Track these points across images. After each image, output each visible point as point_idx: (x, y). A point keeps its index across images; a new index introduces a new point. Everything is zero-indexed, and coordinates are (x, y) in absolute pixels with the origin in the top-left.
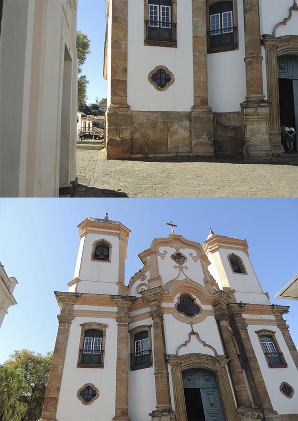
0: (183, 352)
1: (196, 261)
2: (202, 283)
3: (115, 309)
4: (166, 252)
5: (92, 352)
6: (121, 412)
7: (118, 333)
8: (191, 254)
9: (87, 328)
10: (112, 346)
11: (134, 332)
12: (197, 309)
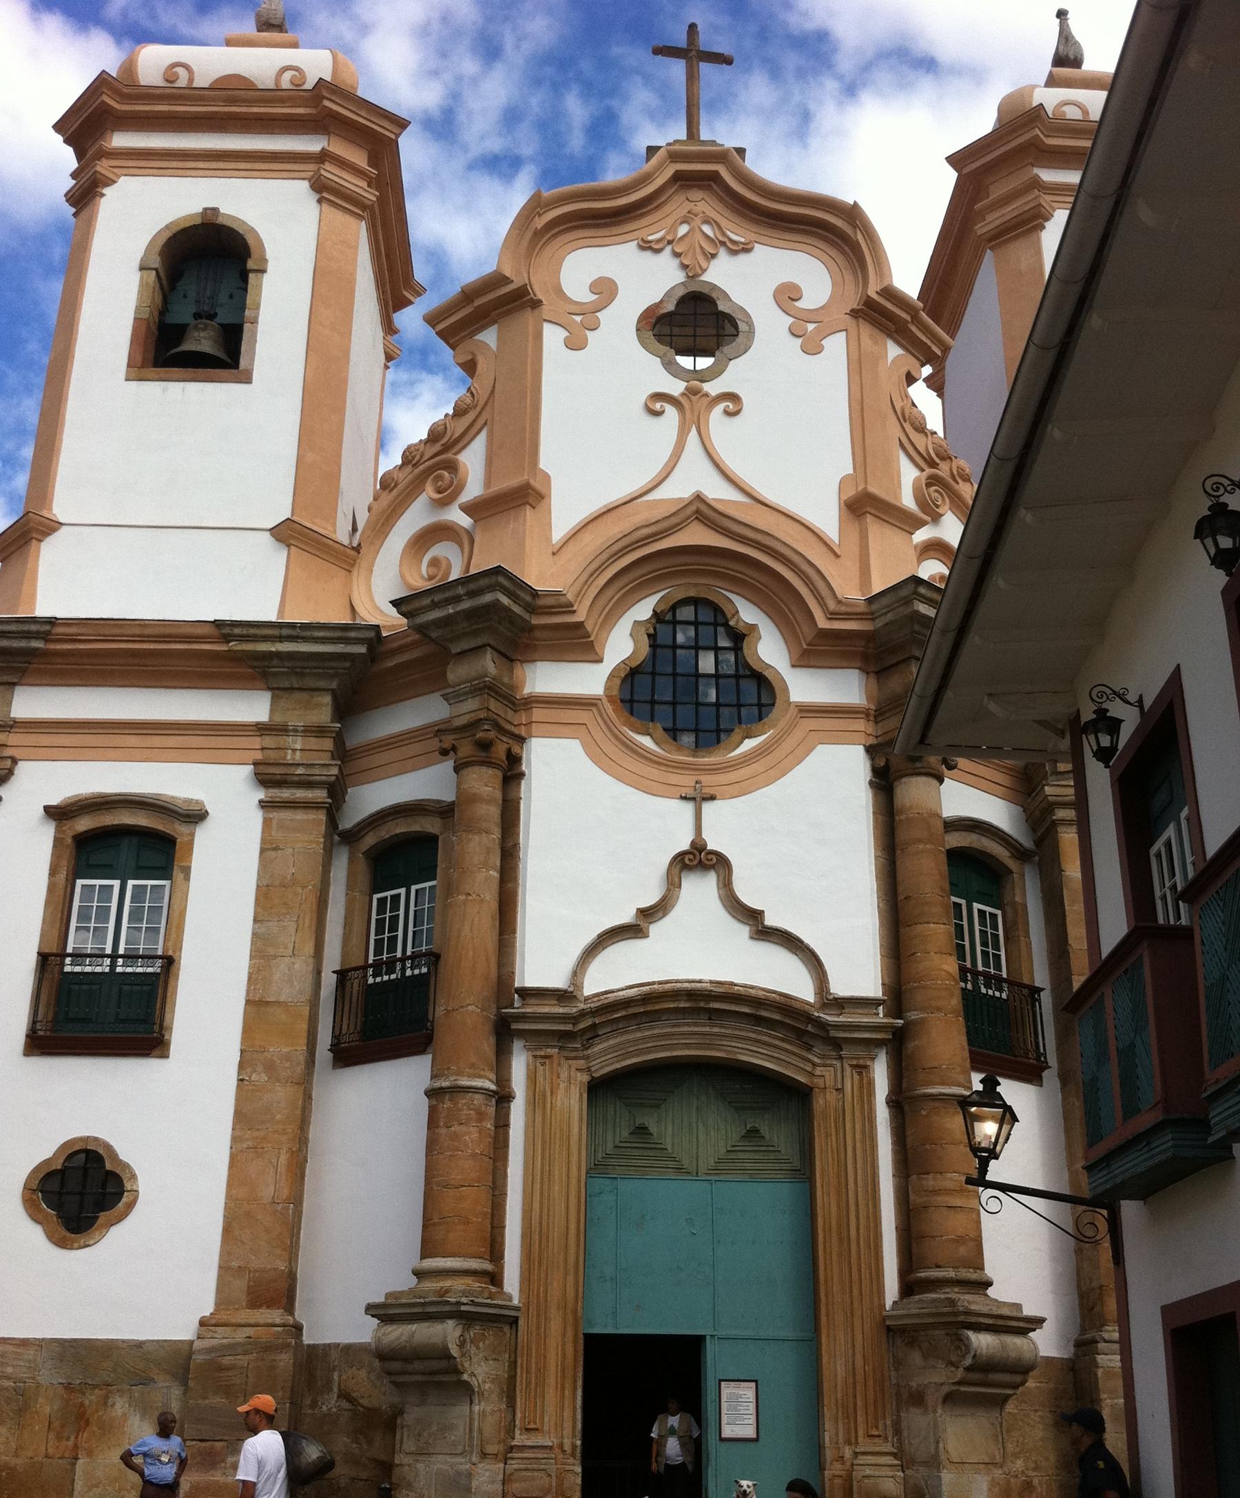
0: (621, 972)
1: (812, 348)
2: (826, 516)
3: (252, 707)
4: (605, 290)
5: (113, 965)
6: (250, 1291)
7: (262, 851)
8: (787, 296)
9: (84, 824)
10: (219, 925)
11: (370, 840)
12: (754, 695)
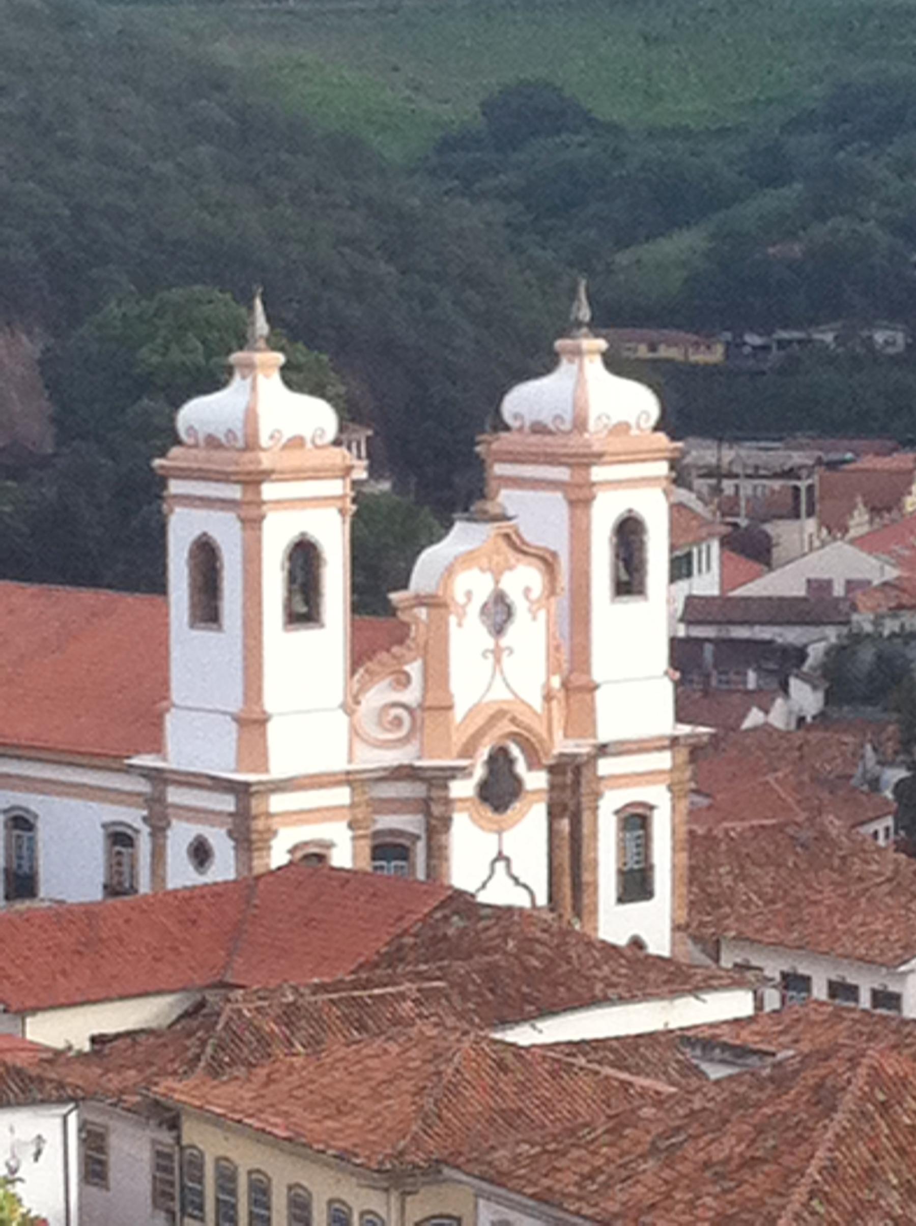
1: (534, 618)
2: (537, 704)
4: (469, 594)
